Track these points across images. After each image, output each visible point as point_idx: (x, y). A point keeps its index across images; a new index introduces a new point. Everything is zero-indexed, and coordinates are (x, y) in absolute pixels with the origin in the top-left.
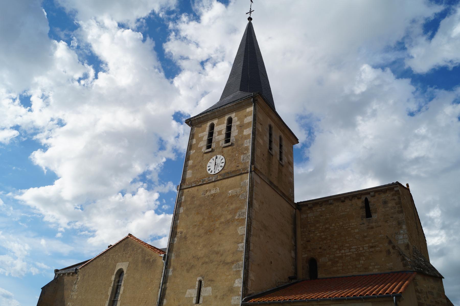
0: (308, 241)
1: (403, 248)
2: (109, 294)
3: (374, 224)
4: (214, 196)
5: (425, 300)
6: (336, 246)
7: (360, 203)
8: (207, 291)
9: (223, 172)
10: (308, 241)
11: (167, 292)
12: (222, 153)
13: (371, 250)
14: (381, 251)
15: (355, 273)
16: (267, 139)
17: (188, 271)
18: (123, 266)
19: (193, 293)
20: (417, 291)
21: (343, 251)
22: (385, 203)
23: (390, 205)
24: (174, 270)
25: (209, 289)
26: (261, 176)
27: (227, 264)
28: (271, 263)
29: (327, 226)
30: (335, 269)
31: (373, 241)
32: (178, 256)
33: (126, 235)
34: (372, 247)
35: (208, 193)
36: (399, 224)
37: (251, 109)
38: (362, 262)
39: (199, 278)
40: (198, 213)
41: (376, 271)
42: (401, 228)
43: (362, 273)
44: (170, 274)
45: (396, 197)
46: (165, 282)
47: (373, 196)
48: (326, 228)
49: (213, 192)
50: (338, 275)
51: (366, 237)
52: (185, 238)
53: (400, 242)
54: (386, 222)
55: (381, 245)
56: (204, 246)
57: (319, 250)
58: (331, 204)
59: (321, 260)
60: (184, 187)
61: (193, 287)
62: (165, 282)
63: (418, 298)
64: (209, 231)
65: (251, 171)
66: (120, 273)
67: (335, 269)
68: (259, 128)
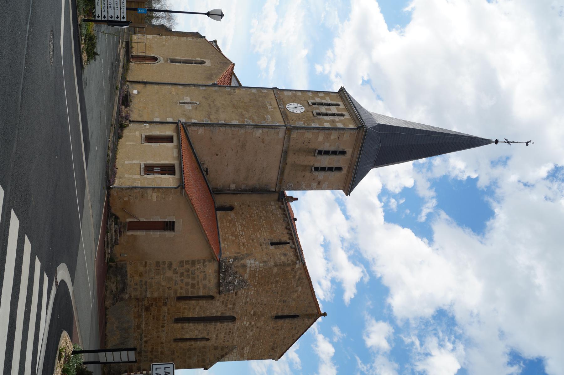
0: (249, 206)
1: (242, 262)
2: (186, 58)
3: (264, 246)
4: (266, 107)
5: (198, 269)
6: (244, 223)
7: (285, 238)
8: (189, 107)
9: (287, 112)
10: (249, 206)
11: (188, 88)
12: (306, 111)
13: (241, 244)
14: (239, 249)
15: (221, 233)
16: (327, 147)
17: (204, 97)
18: (208, 63)
19: (188, 100)
20: (204, 261)
21: (240, 227)
22: (285, 255)
23: (282, 258)
24: (205, 90)
25: (191, 108)
26: (286, 139)
27: (209, 116)
28: (217, 155)
29: (263, 218)
30: (225, 221)
31: (249, 245)
32: (215, 91)
33: (233, 62)
34: (244, 244)
35: (268, 105)
36: (264, 262)
37: (352, 126)
38: (231, 237)
39: (198, 103)
40: (251, 100)
41: (222, 245)
42: (261, 263)
43: (221, 237)
44: (201, 88)
45: (290, 262)
46: (194, 85)
47: (291, 247)
48: (261, 217)
49: (269, 107)
50: (219, 223)
51: (253, 241)
52: (230, 94)
53: (248, 261)
54: (267, 254)
55: (245, 249)
56: (223, 104)
57: (241, 213)
58: (284, 220)
59: (232, 214)
60: (275, 91)
61: (191, 100)
62: (194, 85)
63: (199, 262)
64: (235, 106)
65: (286, 126)
66: (202, 63)
67: (225, 221)
68: (334, 135)
